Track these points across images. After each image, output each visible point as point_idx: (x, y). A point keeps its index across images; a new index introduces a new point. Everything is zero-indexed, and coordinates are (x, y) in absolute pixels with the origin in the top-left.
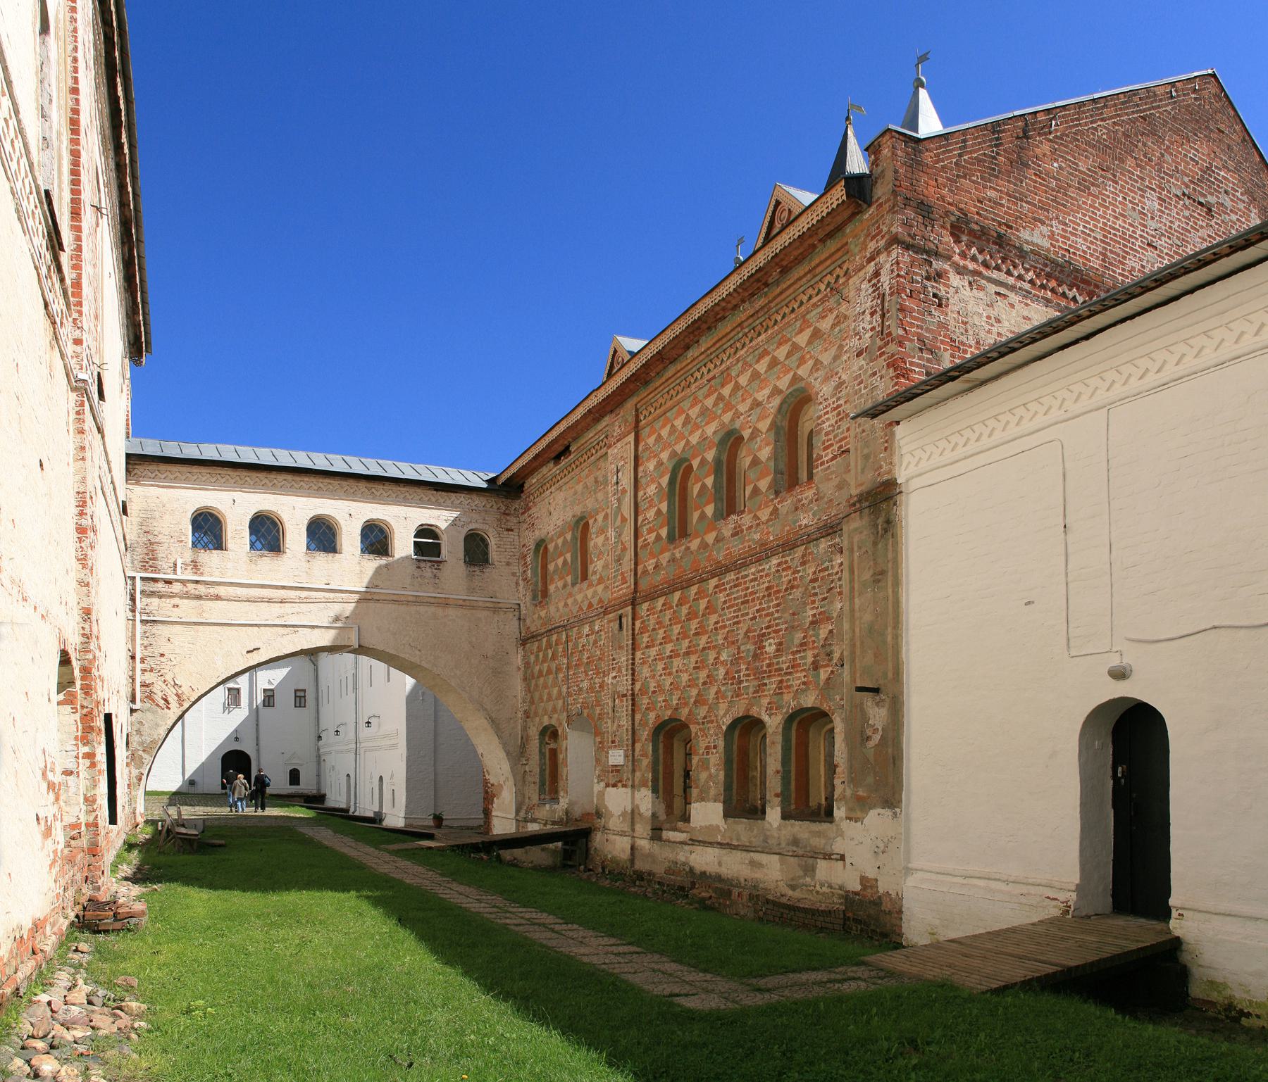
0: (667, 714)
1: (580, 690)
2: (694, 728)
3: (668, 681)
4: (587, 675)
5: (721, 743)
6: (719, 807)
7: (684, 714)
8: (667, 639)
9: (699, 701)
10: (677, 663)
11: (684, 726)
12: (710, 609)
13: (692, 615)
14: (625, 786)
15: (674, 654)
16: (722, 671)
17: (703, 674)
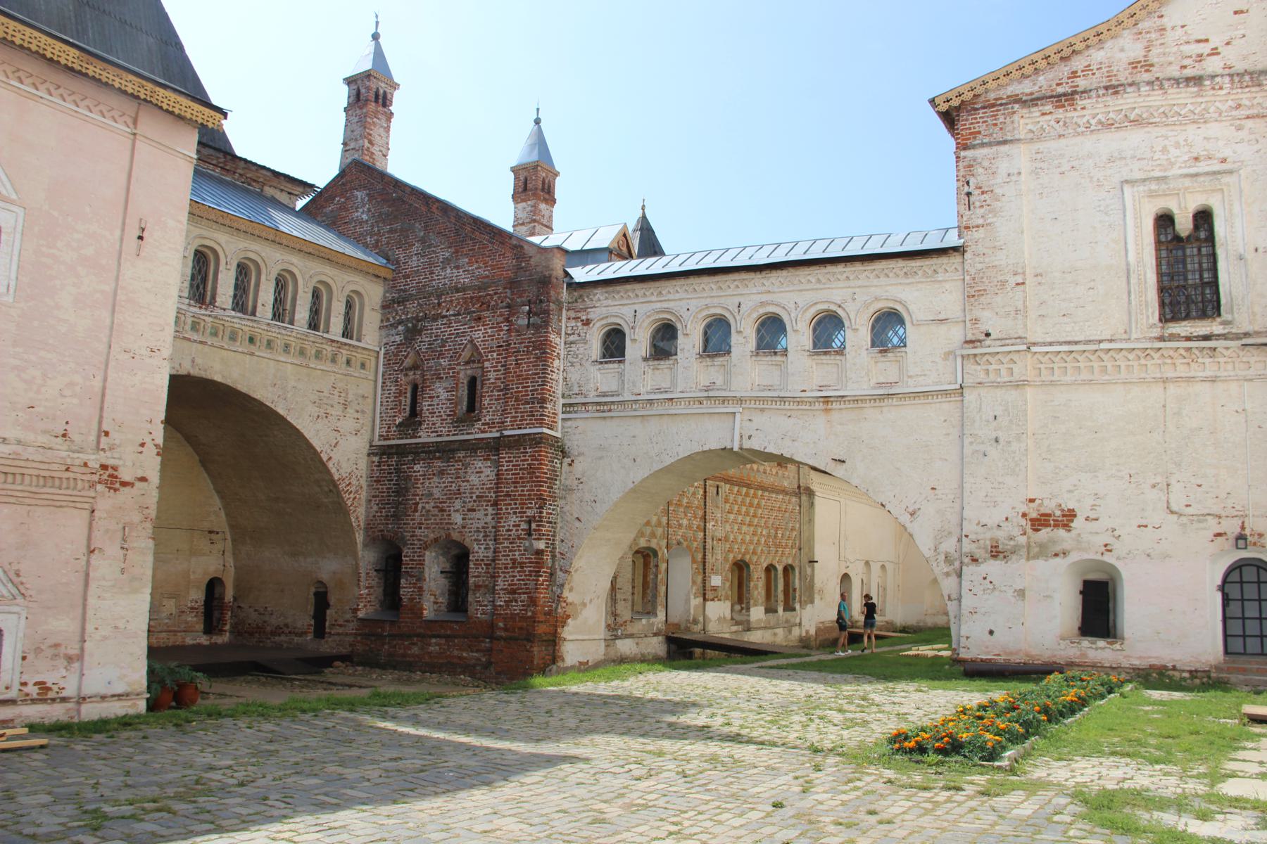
0: (739, 557)
1: (680, 525)
2: (752, 567)
3: (740, 537)
4: (686, 515)
5: (763, 576)
6: (762, 609)
7: (747, 558)
8: (739, 512)
9: (754, 553)
10: (744, 528)
11: (748, 566)
12: (759, 506)
13: (751, 505)
14: (719, 600)
15: (742, 523)
16: (763, 540)
17: (756, 539)
